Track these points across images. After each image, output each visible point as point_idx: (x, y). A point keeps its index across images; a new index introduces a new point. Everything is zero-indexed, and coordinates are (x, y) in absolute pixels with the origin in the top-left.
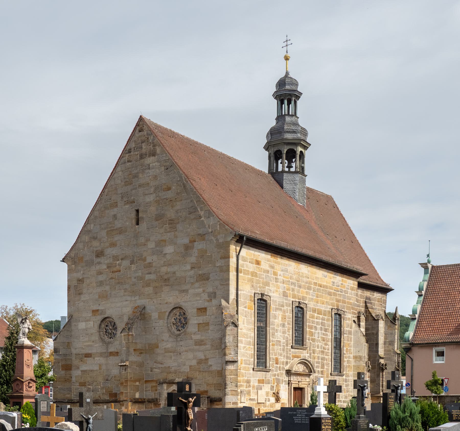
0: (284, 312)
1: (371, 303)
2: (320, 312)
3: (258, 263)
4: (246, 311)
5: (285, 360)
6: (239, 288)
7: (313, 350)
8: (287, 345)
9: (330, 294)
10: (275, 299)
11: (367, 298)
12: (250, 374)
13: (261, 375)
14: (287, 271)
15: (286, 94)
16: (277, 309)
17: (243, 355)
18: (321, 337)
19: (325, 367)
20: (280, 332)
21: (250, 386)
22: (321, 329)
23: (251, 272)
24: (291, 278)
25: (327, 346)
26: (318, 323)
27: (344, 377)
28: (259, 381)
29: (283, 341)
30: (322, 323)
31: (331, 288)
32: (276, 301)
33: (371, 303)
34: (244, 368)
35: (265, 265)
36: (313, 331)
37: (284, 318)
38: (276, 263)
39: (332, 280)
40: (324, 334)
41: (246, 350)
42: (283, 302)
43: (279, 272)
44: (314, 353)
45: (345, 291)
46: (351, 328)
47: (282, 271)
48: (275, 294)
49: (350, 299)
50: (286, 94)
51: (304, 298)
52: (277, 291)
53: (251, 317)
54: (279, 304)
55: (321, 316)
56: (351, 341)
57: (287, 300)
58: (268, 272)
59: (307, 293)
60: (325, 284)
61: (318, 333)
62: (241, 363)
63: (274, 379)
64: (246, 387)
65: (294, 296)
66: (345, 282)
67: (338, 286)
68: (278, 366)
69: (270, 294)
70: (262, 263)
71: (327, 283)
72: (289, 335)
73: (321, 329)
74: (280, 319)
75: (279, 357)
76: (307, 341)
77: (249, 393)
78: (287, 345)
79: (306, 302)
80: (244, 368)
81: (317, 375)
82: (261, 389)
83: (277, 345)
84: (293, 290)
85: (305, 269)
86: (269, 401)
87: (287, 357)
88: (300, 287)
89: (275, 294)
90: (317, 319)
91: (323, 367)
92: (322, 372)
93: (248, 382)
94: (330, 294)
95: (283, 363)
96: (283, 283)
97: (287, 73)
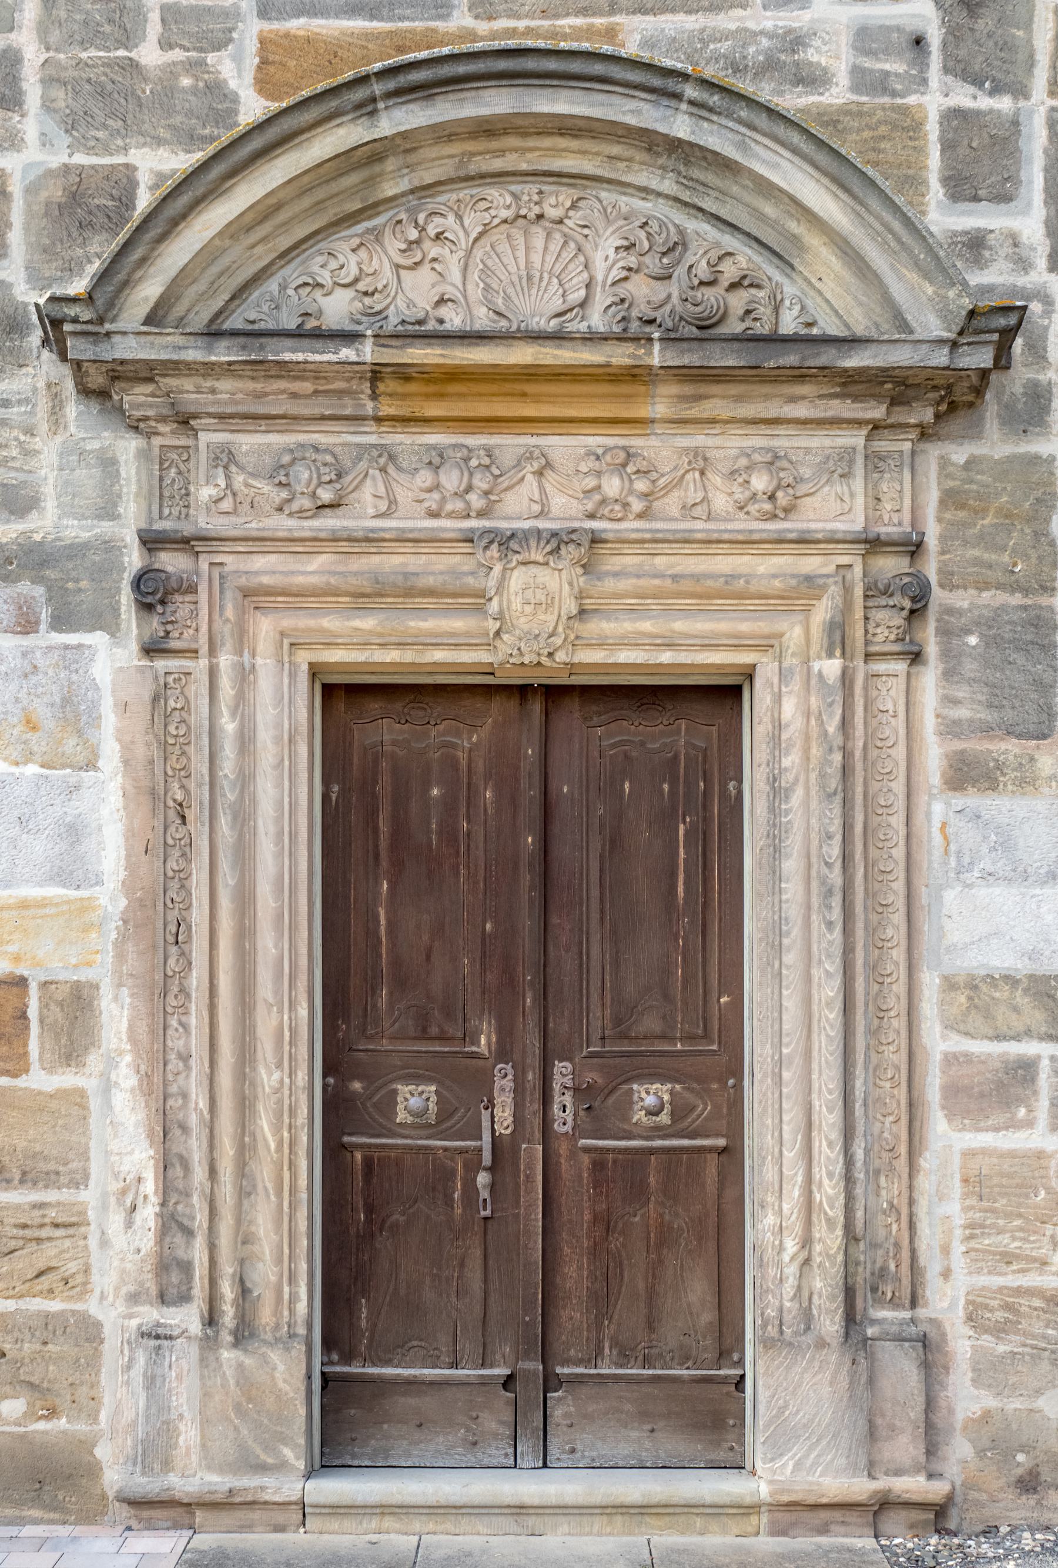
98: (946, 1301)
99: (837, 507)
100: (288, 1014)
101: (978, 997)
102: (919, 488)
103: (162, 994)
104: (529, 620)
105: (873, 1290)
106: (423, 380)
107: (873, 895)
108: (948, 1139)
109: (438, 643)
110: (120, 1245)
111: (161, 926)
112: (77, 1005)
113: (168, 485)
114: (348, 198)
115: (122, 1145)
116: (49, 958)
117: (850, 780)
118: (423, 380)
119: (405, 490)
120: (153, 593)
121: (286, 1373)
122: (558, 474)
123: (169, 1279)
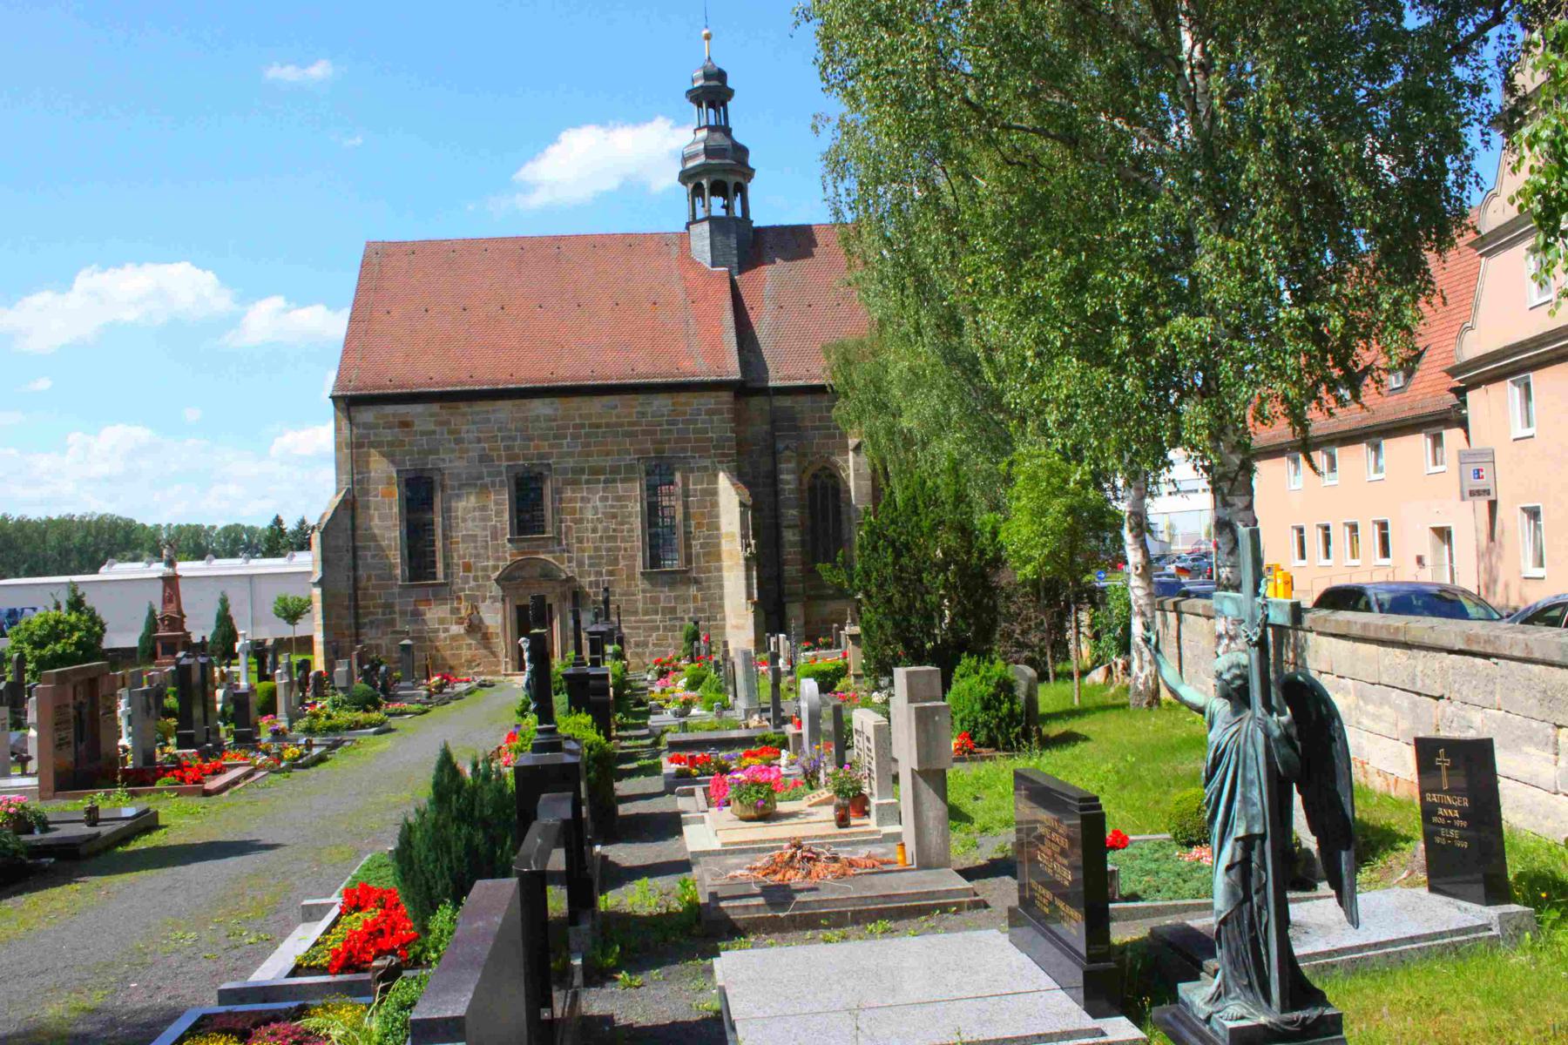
3: (405, 424)
5: (491, 563)
8: (494, 537)
14: (488, 421)
19: (622, 563)
20: (474, 520)
24: (500, 430)
29: (479, 532)
31: (631, 424)
34: (375, 587)
40: (612, 507)
43: (464, 428)
44: (580, 541)
47: (474, 423)
51: (541, 456)
55: (602, 478)
58: (434, 432)
59: (551, 446)
65: (516, 457)
66: (686, 404)
69: (442, 465)
71: (618, 416)
77: (392, 623)
86: (446, 630)
88: (530, 439)
91: (615, 561)
93: (389, 607)
95: (485, 569)
96: (479, 440)
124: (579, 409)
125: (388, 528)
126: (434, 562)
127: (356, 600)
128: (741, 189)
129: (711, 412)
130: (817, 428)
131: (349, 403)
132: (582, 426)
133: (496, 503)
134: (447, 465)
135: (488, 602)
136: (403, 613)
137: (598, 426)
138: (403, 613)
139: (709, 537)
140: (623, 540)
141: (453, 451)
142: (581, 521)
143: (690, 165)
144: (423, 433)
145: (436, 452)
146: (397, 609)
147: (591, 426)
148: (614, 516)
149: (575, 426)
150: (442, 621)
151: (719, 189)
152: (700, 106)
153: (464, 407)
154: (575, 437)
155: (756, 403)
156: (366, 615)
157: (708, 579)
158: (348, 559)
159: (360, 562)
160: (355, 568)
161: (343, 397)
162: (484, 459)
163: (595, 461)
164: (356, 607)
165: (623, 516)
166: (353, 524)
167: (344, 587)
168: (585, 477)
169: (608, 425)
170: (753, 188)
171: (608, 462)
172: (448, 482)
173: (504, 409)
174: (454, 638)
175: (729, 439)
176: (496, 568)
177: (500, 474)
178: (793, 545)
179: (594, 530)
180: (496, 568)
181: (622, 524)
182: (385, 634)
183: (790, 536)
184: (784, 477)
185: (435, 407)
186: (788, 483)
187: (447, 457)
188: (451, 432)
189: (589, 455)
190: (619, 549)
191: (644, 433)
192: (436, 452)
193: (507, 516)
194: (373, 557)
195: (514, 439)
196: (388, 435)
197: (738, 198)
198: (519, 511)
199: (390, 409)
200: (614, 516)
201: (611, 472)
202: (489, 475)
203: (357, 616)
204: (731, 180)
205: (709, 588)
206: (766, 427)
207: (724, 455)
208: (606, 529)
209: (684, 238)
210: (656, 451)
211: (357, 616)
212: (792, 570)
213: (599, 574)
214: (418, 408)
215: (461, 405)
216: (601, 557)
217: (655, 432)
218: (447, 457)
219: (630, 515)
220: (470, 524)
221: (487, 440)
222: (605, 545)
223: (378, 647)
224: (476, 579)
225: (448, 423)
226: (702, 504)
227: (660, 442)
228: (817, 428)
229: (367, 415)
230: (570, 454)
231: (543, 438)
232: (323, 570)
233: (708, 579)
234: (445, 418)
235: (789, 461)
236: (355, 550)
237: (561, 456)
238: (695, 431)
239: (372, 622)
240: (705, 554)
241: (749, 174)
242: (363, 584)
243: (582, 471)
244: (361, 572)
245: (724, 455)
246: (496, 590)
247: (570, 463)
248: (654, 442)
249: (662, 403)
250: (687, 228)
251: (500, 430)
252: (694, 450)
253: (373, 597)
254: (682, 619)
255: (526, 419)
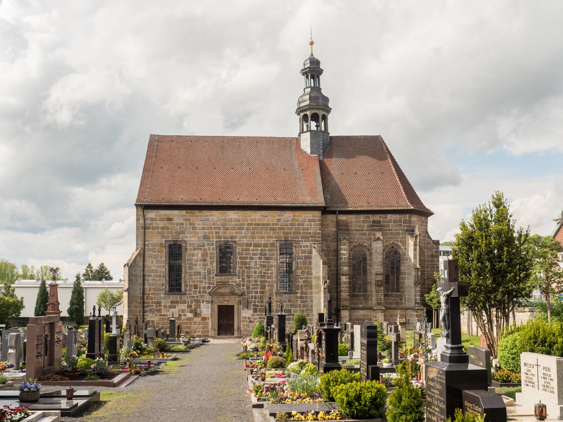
0: (206, 250)
1: (381, 226)
2: (256, 245)
3: (170, 219)
4: (154, 255)
5: (207, 285)
6: (146, 239)
7: (247, 276)
8: (209, 274)
9: (274, 229)
10: (192, 242)
11: (373, 222)
12: (160, 297)
13: (173, 297)
14: (208, 220)
15: (313, 71)
16: (194, 250)
17: (153, 285)
18: (260, 265)
19: (267, 288)
20: (200, 265)
21: (160, 306)
22: (260, 258)
23: (161, 227)
24: (213, 224)
25: (270, 271)
26: (253, 254)
27: (299, 295)
28: (172, 302)
29: (202, 271)
30: (261, 254)
31: (273, 224)
32: (194, 244)
33: (381, 226)
34: (152, 294)
35: (176, 221)
36: (248, 261)
37: (205, 255)
38: (192, 216)
39: (277, 218)
40: (264, 262)
41: (156, 281)
42: (204, 243)
43: (197, 223)
45: (298, 225)
46: (310, 252)
47: (201, 221)
48: (193, 239)
49: (308, 230)
50: (313, 71)
51: (232, 237)
52: (195, 236)
53: (161, 258)
54: (198, 246)
55: (260, 248)
56: (310, 263)
57: (209, 241)
58: (182, 224)
59: (237, 233)
60: (266, 222)
61: (256, 262)
62: (150, 291)
63: (192, 300)
64: (156, 306)
65: (221, 237)
66: (298, 216)
67: (288, 221)
68: (198, 290)
70: (175, 219)
71: (268, 221)
72: (214, 266)
73: (260, 258)
74: (200, 255)
75: (199, 284)
76: (238, 269)
77: (160, 311)
78: (209, 274)
79: (236, 240)
80: (152, 294)
81: (253, 294)
82: (175, 307)
83: (195, 275)
84: (217, 233)
85: (232, 215)
86: (185, 315)
87: (210, 283)
88: (227, 229)
89: (193, 239)
90: (253, 250)
91: (263, 287)
92: (262, 292)
93: (159, 303)
94: (274, 229)
95: (204, 288)
96: (204, 229)
97: (312, 55)
98: (242, 329)
99: (237, 299)
100: (217, 318)
101: (243, 318)
102: (241, 298)
103: (212, 318)
104: (226, 303)
105: (239, 328)
106: (223, 295)
107: (239, 314)
108: (242, 323)
109: (222, 304)
110: (210, 327)
111: (212, 315)
112: (208, 318)
113: (212, 298)
114: (219, 288)
115: (210, 323)
116: (207, 316)
117: (238, 309)
118: (223, 295)
119: (221, 299)
120: (212, 302)
121: (216, 332)
122: (227, 298)
123: (212, 328)
124: (251, 216)
125: (160, 267)
126: (181, 284)
127: (144, 299)
128: (325, 118)
129: (310, 221)
130: (358, 230)
131: (144, 207)
132: (251, 224)
133: (210, 258)
134: (188, 239)
135: (205, 303)
136: (165, 306)
137: (259, 225)
138: (165, 306)
139: (307, 278)
140: (268, 277)
141: (192, 233)
142: (249, 268)
143: (302, 105)
144: (178, 224)
145: (184, 233)
146: (163, 304)
147: (255, 225)
148: (264, 266)
149: (248, 224)
150: (183, 311)
151: (315, 117)
152: (307, 77)
153: (197, 212)
154: (247, 229)
155: (331, 218)
156: (148, 306)
157: (306, 297)
158: (141, 281)
159: (146, 282)
160: (144, 284)
161: (141, 205)
162: (206, 237)
163: (256, 241)
164: (144, 303)
165: (268, 266)
166: (144, 265)
167: (138, 292)
168: (251, 248)
169: (263, 225)
170: (330, 117)
171: (263, 242)
172: (188, 247)
173: (216, 215)
174: (189, 319)
175: (319, 233)
176: (209, 288)
177: (212, 245)
178: (345, 283)
179: (255, 273)
180: (209, 288)
181: (268, 270)
182: (156, 315)
183: (344, 279)
184: (342, 252)
185: (184, 212)
186: (344, 255)
187: (188, 236)
188: (190, 224)
189: (254, 238)
190: (266, 281)
191: (280, 229)
192: (184, 233)
193: (215, 264)
194: (152, 280)
195: (219, 229)
196: (161, 224)
197: (323, 123)
198: (221, 262)
199: (163, 212)
200: (264, 266)
201: (264, 247)
202: (208, 245)
203: (144, 307)
204: (321, 113)
205: (307, 301)
206: (334, 229)
207: (315, 240)
208: (261, 272)
209: (298, 140)
210: (285, 237)
211: (144, 307)
212: (345, 295)
213: (257, 292)
214: (176, 212)
215: (196, 211)
216: (258, 285)
217: (284, 229)
218: (188, 236)
219: (272, 266)
220: (198, 267)
221: (207, 229)
222: (259, 279)
223: (153, 322)
224: (199, 292)
225: (190, 220)
226: (305, 263)
227: (287, 233)
228: (358, 230)
229: (151, 214)
230: (245, 237)
231: (233, 229)
232: (129, 284)
233: (306, 297)
234: (188, 217)
235: (345, 245)
236: (144, 276)
237: (242, 237)
238: (303, 229)
239: (150, 310)
240: (305, 286)
241: (328, 110)
242: (147, 292)
243: (250, 245)
244: (146, 287)
245: (315, 240)
246: (208, 297)
247: (245, 241)
248: (284, 233)
249: (288, 215)
250: (299, 135)
251: (213, 224)
252: (302, 237)
253: (152, 299)
254: (294, 315)
255: (226, 220)
